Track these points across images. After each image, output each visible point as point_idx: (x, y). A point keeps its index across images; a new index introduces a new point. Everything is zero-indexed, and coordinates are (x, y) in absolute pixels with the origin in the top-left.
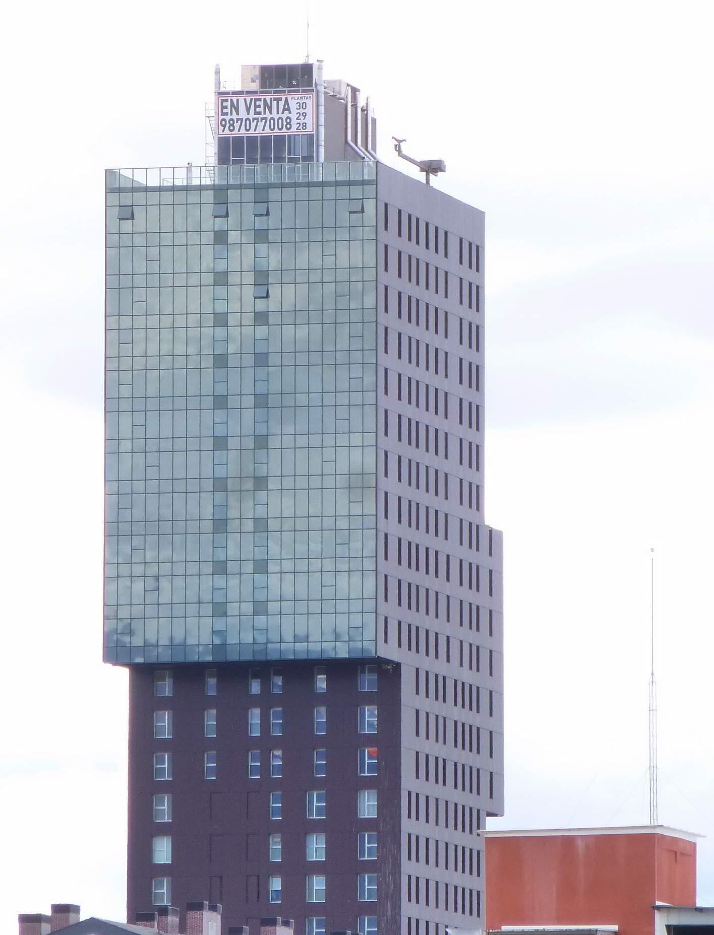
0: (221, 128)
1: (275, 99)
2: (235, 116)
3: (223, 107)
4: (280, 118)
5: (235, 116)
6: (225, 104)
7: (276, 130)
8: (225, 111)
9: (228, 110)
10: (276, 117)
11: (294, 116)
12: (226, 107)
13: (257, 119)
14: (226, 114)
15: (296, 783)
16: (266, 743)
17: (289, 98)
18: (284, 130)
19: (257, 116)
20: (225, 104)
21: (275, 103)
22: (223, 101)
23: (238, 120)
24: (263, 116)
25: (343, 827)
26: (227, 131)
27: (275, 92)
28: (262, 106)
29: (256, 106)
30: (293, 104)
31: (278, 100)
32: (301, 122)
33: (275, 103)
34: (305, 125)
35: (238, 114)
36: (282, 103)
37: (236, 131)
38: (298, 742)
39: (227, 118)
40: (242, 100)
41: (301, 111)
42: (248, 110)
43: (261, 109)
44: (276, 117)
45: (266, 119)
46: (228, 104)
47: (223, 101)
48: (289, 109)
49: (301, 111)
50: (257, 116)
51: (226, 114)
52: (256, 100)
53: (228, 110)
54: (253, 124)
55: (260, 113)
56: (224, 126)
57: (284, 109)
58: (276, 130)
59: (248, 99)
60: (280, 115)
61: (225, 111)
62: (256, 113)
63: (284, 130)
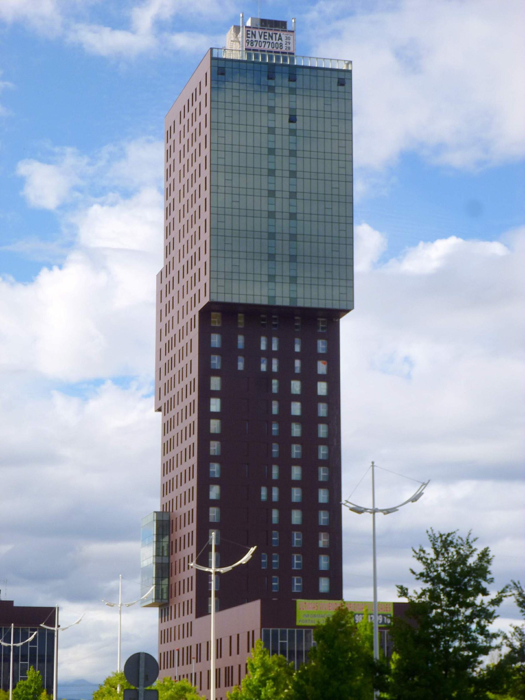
0: (247, 44)
2: (254, 39)
3: (248, 34)
4: (276, 43)
5: (254, 39)
6: (249, 32)
7: (275, 48)
8: (249, 36)
9: (250, 36)
10: (275, 42)
11: (284, 42)
12: (249, 34)
14: (249, 37)
15: (286, 375)
16: (269, 354)
17: (282, 34)
18: (279, 49)
20: (249, 32)
21: (274, 35)
22: (248, 31)
23: (255, 41)
26: (249, 45)
29: (265, 36)
30: (283, 37)
31: (276, 34)
32: (288, 46)
33: (274, 35)
34: (289, 48)
35: (255, 38)
36: (278, 36)
37: (254, 46)
38: (286, 356)
39: (250, 39)
41: (288, 41)
42: (261, 37)
43: (267, 37)
44: (275, 42)
45: (270, 42)
46: (250, 33)
47: (248, 31)
48: (281, 39)
49: (288, 41)
51: (249, 37)
52: (265, 33)
53: (250, 36)
54: (263, 44)
55: (266, 39)
56: (248, 43)
57: (279, 39)
58: (275, 48)
59: (261, 32)
60: (277, 41)
61: (249, 36)
62: (264, 39)
63: (279, 49)
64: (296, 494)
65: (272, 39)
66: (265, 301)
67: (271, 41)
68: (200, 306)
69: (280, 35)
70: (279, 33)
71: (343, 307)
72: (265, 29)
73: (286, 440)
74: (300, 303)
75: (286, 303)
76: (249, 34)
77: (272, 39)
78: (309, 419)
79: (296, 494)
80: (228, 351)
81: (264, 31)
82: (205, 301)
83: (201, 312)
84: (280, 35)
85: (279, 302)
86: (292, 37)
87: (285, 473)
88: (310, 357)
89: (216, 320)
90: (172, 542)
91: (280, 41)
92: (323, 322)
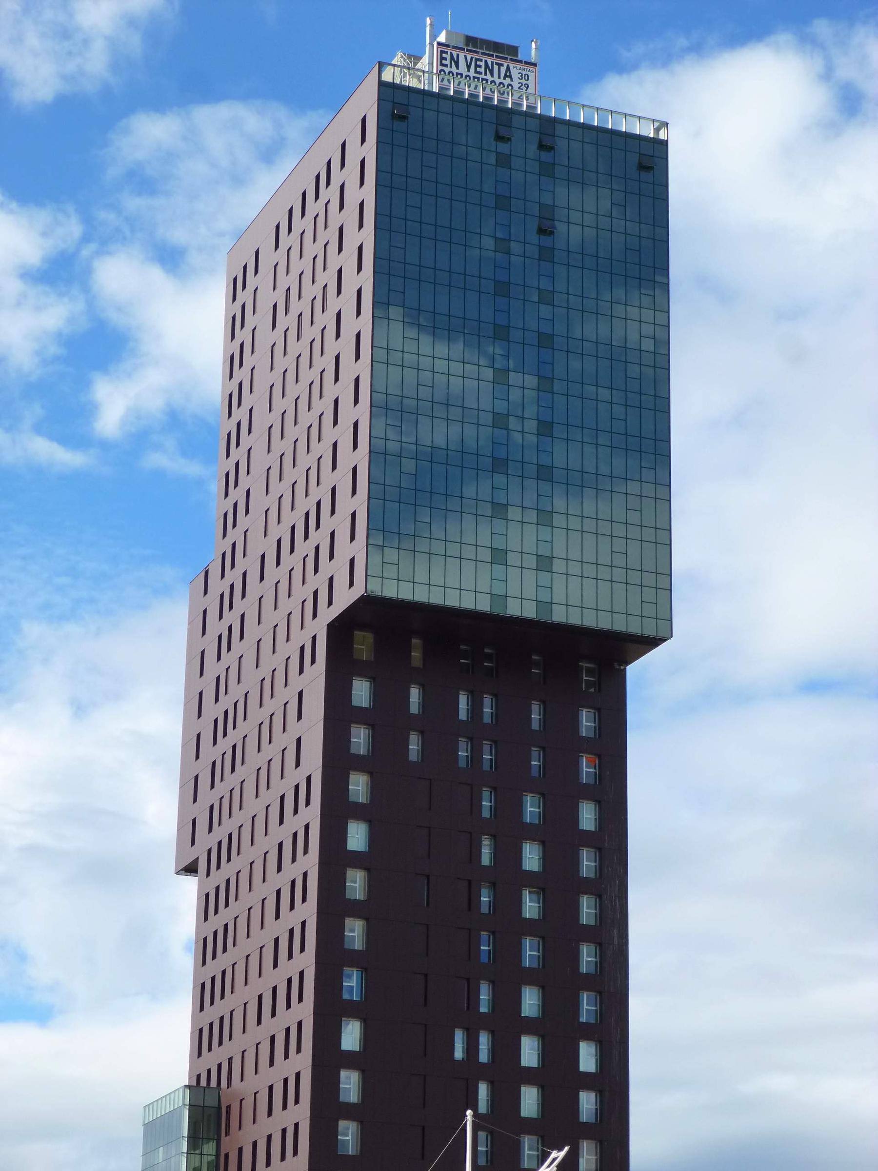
1: (497, 64)
3: (442, 59)
4: (501, 83)
9: (447, 62)
10: (498, 81)
13: (478, 79)
14: (446, 66)
16: (474, 730)
17: (511, 66)
19: (477, 75)
20: (444, 55)
21: (496, 67)
24: (483, 76)
25: (560, 837)
27: (497, 57)
28: (483, 67)
29: (477, 66)
30: (515, 73)
31: (500, 65)
33: (496, 67)
35: (458, 68)
36: (503, 69)
39: (447, 70)
40: (462, 56)
43: (482, 70)
44: (498, 81)
45: (487, 80)
47: (442, 52)
48: (510, 77)
49: (523, 81)
50: (477, 75)
51: (446, 66)
52: (477, 60)
53: (447, 62)
55: (481, 73)
57: (505, 77)
60: (501, 80)
61: (444, 62)
62: (476, 72)
64: (530, 1052)
65: (492, 75)
66: (484, 605)
67: (489, 77)
68: (328, 614)
69: (508, 68)
70: (505, 65)
71: (649, 630)
72: (478, 53)
73: (508, 926)
74: (559, 616)
75: (530, 612)
76: (445, 59)
77: (492, 75)
78: (559, 885)
79: (530, 1052)
80: (385, 718)
81: (475, 56)
82: (345, 598)
83: (332, 627)
84: (508, 68)
85: (513, 609)
86: (532, 76)
87: (507, 1000)
88: (562, 744)
89: (363, 645)
90: (227, 1155)
91: (508, 81)
92: (590, 672)
